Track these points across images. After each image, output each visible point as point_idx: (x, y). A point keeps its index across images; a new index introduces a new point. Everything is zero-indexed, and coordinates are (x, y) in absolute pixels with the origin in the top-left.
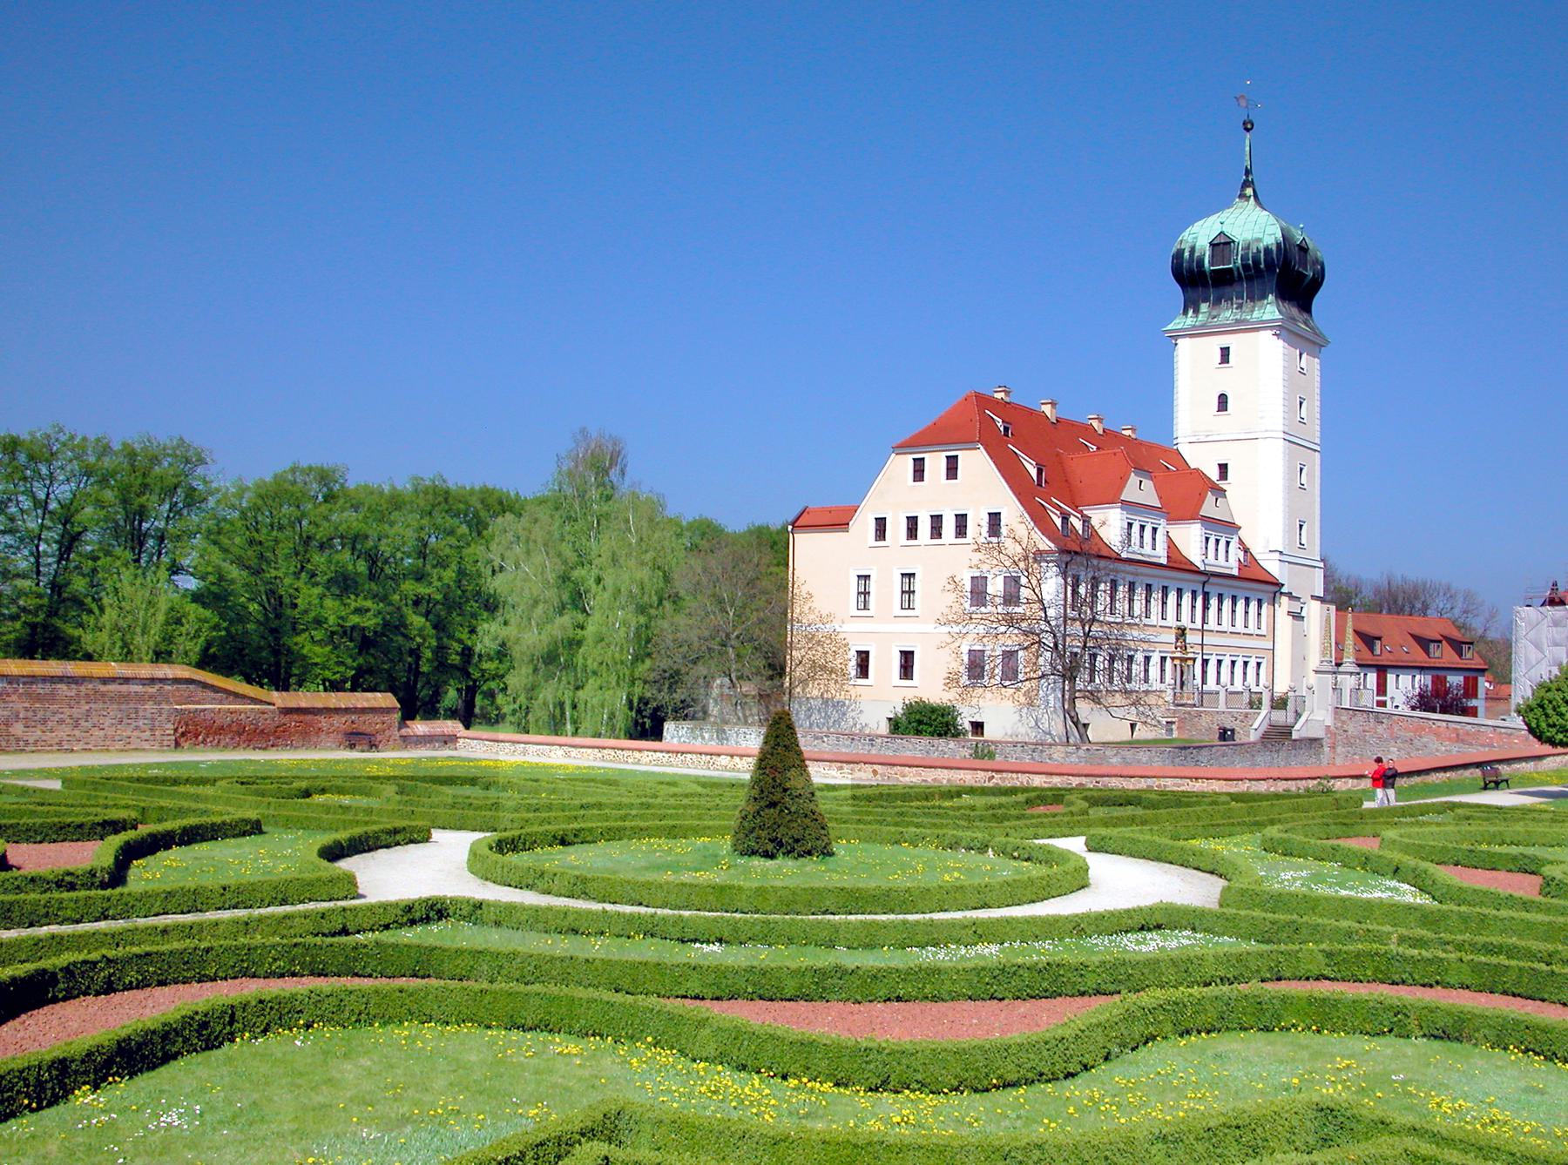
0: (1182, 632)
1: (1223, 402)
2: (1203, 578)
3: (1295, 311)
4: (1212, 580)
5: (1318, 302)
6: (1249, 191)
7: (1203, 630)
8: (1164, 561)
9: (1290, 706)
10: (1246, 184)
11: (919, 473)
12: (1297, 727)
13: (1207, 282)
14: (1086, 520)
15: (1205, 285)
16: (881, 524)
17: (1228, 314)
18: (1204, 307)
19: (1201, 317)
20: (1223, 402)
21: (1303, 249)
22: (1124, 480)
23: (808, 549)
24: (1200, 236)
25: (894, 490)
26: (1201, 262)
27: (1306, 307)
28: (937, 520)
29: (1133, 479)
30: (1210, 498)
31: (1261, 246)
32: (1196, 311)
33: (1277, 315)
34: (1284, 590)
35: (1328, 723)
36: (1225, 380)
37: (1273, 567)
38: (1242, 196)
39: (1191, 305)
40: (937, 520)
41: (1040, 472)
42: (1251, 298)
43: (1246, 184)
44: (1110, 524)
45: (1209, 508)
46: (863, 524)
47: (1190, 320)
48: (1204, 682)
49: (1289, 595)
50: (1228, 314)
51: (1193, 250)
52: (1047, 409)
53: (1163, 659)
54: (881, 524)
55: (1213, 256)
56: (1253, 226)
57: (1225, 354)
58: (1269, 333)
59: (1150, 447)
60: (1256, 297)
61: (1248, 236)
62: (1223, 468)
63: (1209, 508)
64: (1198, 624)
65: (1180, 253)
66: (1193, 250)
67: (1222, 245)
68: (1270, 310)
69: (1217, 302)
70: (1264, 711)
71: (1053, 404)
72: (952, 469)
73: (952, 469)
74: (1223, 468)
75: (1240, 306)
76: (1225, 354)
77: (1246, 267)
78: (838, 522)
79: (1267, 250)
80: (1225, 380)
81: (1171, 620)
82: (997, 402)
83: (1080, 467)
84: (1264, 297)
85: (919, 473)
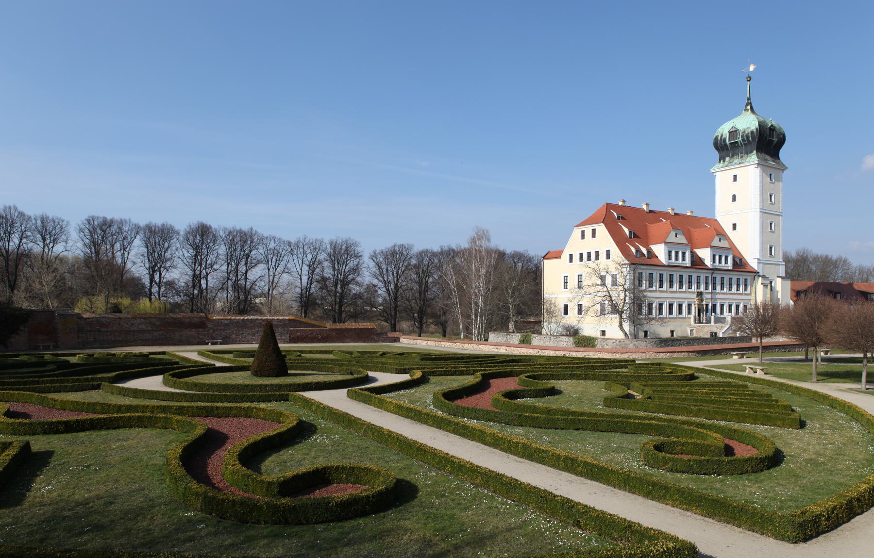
0: (700, 294)
1: (734, 198)
3: (768, 157)
5: (783, 153)
6: (749, 107)
7: (712, 293)
10: (747, 105)
11: (583, 237)
13: (728, 149)
14: (650, 252)
16: (571, 256)
17: (736, 161)
18: (727, 159)
20: (734, 198)
21: (772, 129)
22: (668, 234)
23: (549, 267)
24: (724, 130)
25: (575, 245)
26: (725, 140)
27: (775, 155)
28: (589, 254)
31: (749, 131)
32: (724, 161)
36: (735, 188)
37: (754, 264)
38: (746, 110)
39: (722, 159)
40: (589, 254)
41: (630, 233)
43: (747, 105)
44: (660, 251)
46: (565, 256)
47: (721, 164)
49: (764, 277)
50: (736, 160)
52: (644, 207)
54: (571, 256)
56: (747, 123)
59: (701, 218)
60: (748, 152)
62: (734, 226)
63: (716, 242)
64: (710, 290)
65: (717, 137)
67: (733, 133)
68: (754, 158)
69: (732, 156)
71: (647, 205)
72: (594, 235)
73: (594, 235)
74: (734, 226)
77: (743, 140)
78: (557, 255)
79: (752, 132)
80: (735, 188)
82: (619, 206)
83: (654, 229)
84: (752, 152)
85: (583, 237)
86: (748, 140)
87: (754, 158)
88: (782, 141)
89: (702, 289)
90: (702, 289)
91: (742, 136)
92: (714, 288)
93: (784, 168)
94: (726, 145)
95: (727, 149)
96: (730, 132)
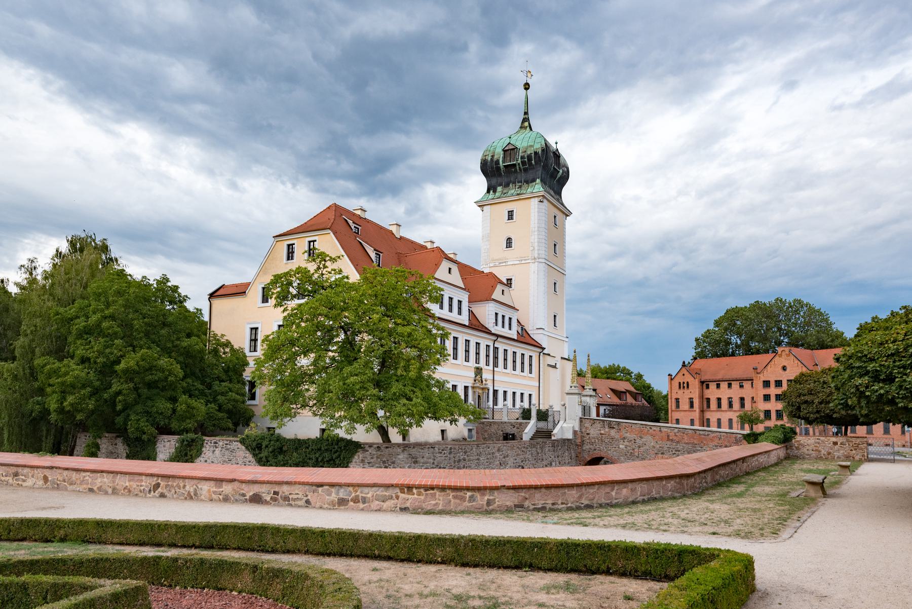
0: (479, 371)
2: (495, 338)
4: (499, 339)
8: (467, 324)
9: (550, 419)
12: (555, 431)
15: (500, 175)
17: (512, 191)
18: (499, 189)
19: (497, 194)
21: (557, 155)
22: (437, 266)
26: (498, 161)
29: (445, 265)
30: (499, 288)
32: (495, 192)
33: (542, 189)
34: (545, 351)
35: (577, 428)
42: (527, 182)
45: (497, 295)
48: (495, 402)
50: (512, 191)
51: (493, 156)
53: (466, 388)
55: (504, 158)
57: (511, 215)
58: (537, 200)
61: (525, 144)
66: (493, 156)
68: (538, 187)
69: (507, 185)
70: (533, 421)
74: (509, 280)
75: (520, 187)
76: (511, 215)
77: (523, 163)
81: (472, 363)
84: (534, 180)
86: (530, 164)
87: (538, 187)
88: (565, 177)
89: (482, 364)
90: (482, 364)
91: (522, 158)
92: (496, 365)
93: (567, 213)
94: (498, 168)
95: (500, 175)
96: (505, 151)
